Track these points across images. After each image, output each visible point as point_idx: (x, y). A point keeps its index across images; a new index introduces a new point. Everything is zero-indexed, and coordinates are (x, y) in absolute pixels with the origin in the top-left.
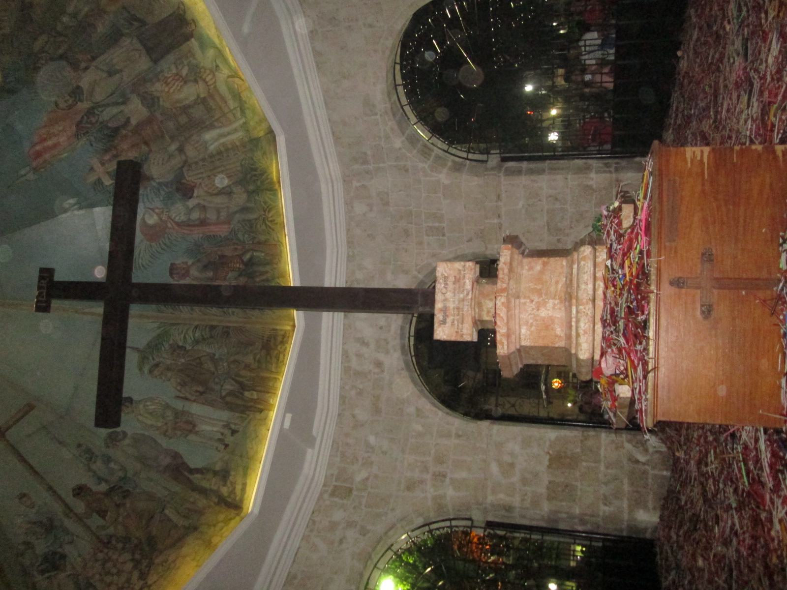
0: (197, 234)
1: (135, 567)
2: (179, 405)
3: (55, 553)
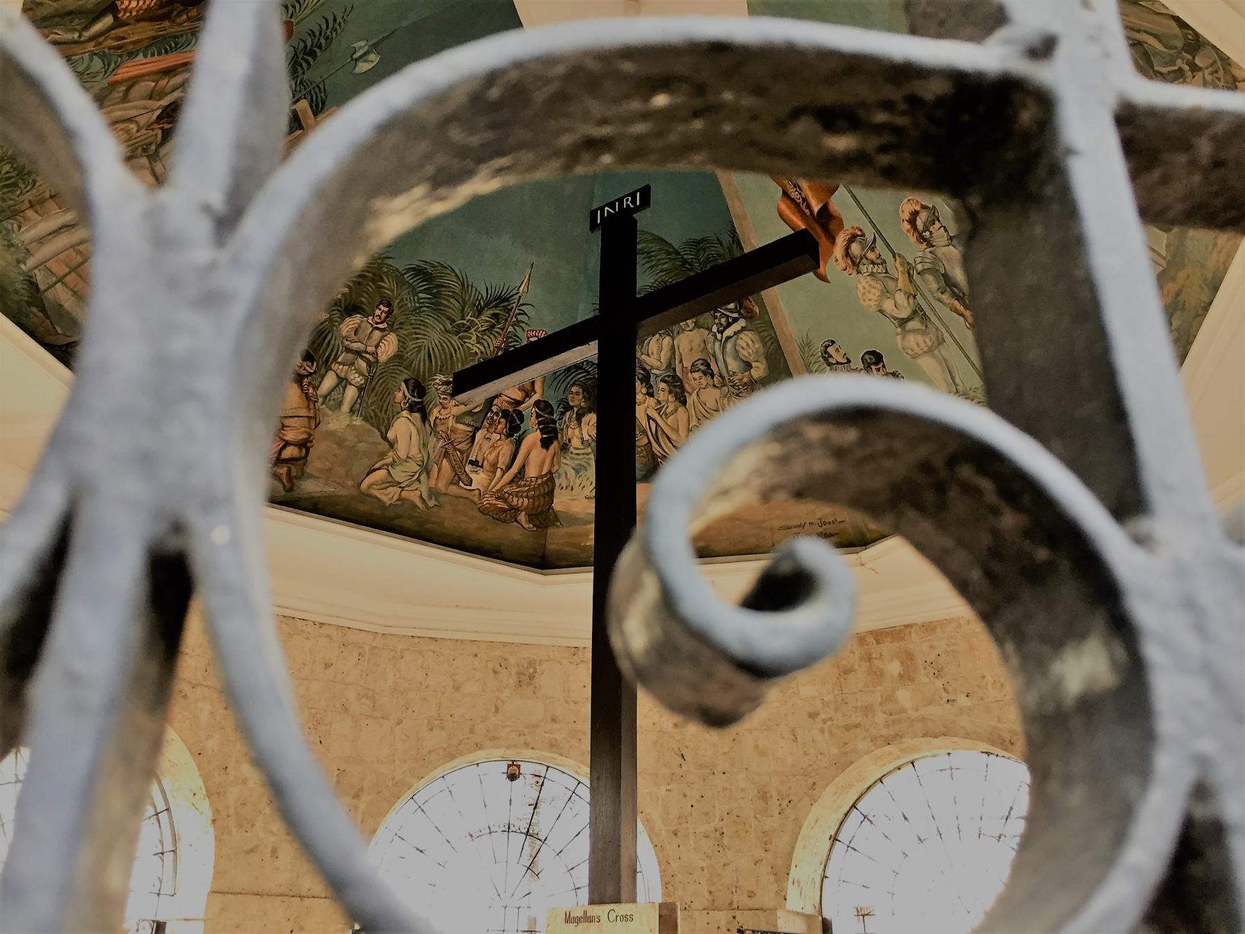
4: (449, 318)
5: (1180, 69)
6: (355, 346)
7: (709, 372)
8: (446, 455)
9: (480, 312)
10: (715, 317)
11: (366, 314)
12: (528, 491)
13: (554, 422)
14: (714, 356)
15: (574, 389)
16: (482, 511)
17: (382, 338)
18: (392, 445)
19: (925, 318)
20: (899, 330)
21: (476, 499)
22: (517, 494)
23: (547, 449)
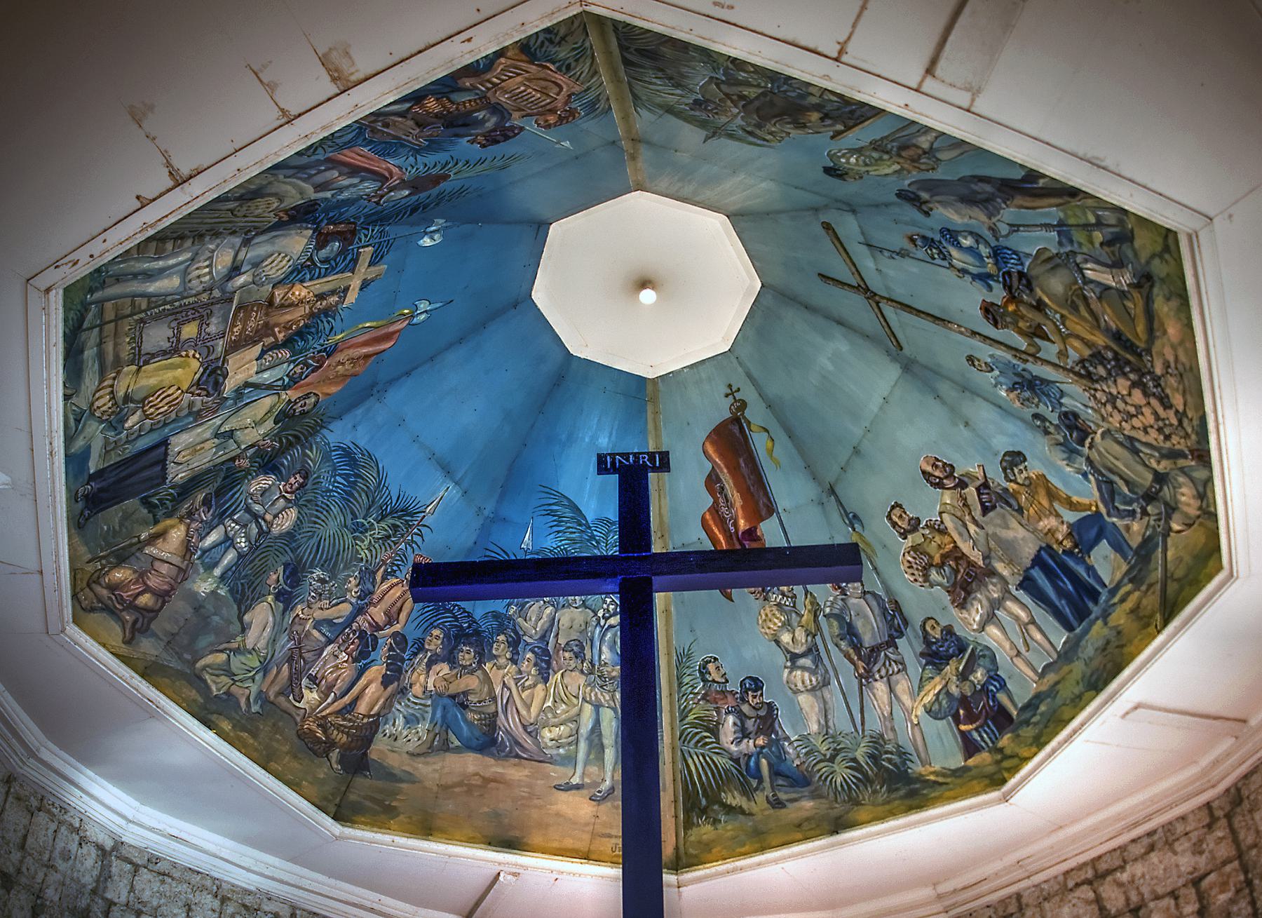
1: (1146, 394)
4: (353, 513)
5: (1134, 511)
6: (257, 508)
7: (579, 655)
8: (290, 660)
9: (383, 518)
10: (605, 602)
11: (281, 478)
12: (351, 728)
13: (403, 660)
14: (592, 641)
15: (436, 632)
16: (301, 735)
17: (284, 509)
18: (244, 629)
19: (818, 660)
20: (789, 664)
21: (298, 719)
23: (385, 688)
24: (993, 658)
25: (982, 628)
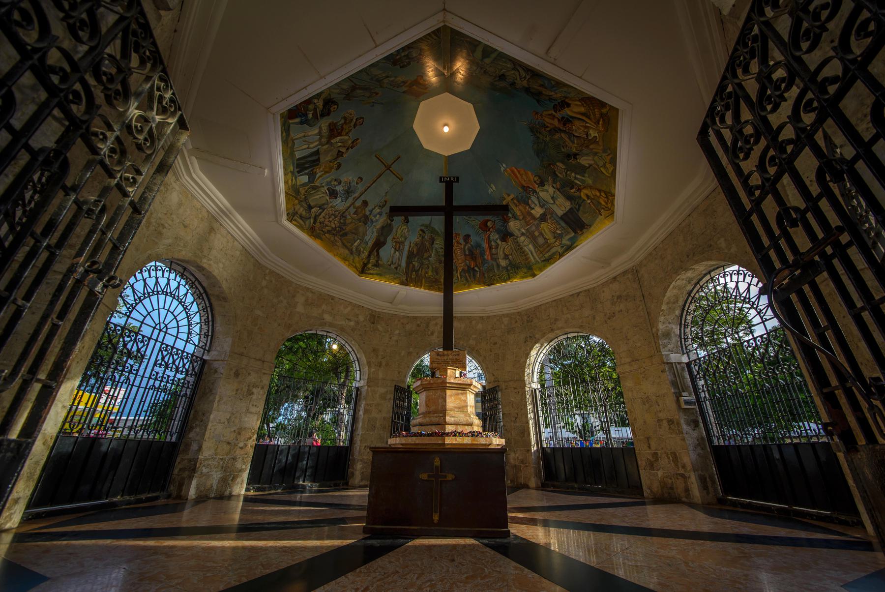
0: (485, 245)
2: (407, 244)
3: (337, 194)
18: (590, 165)
22: (594, 115)
24: (310, 125)
25: (320, 128)
